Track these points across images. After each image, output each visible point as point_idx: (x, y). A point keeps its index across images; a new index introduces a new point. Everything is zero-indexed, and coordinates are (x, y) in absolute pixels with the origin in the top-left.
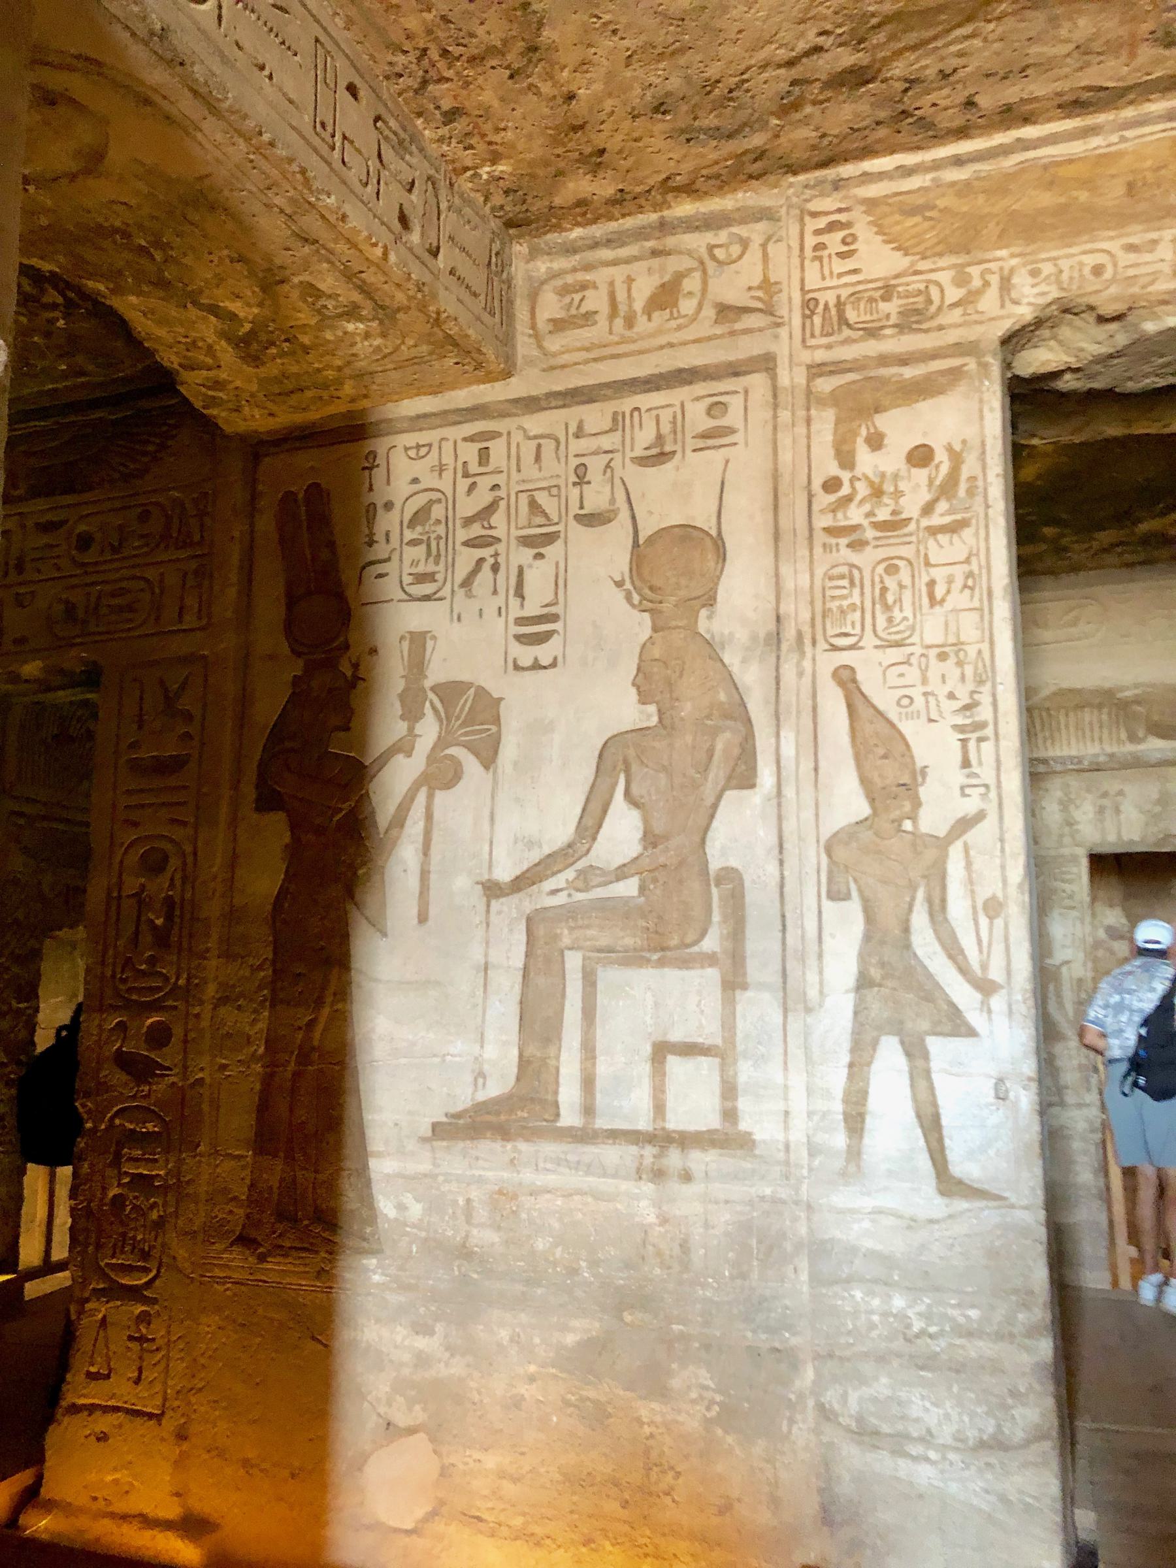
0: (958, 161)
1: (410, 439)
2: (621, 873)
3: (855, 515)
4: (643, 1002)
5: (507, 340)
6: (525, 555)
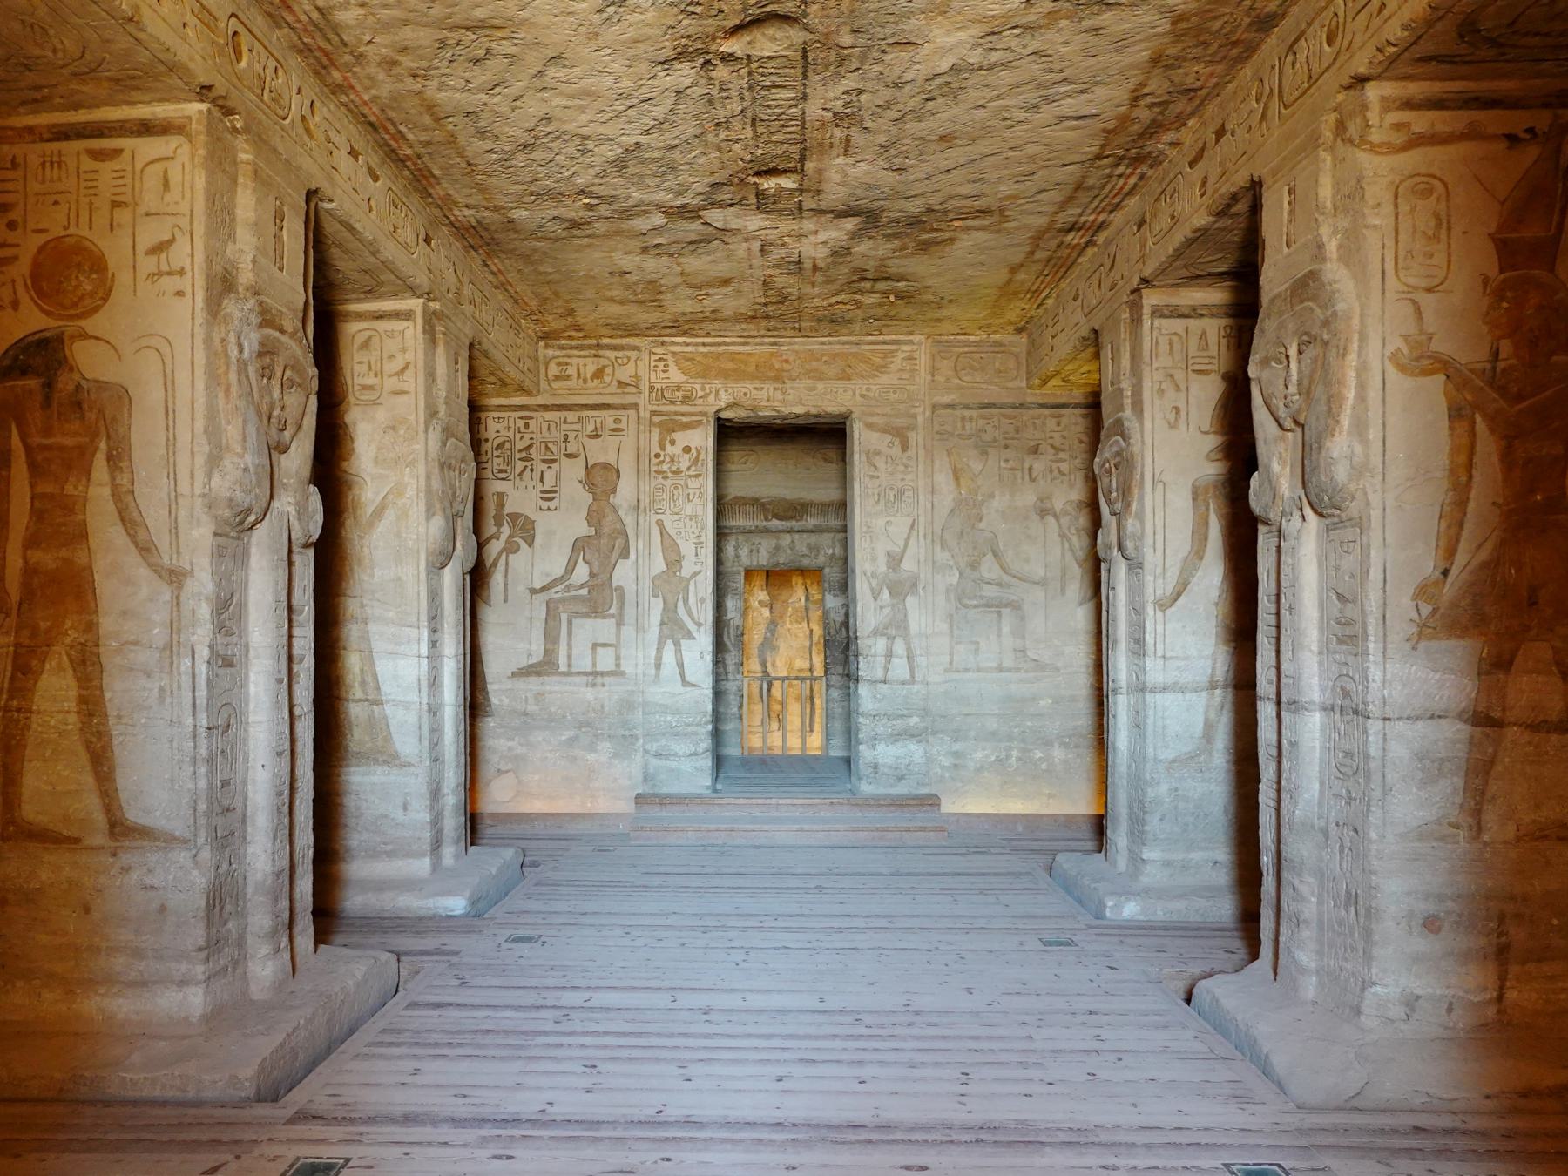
0: (704, 344)
1: (496, 415)
2: (581, 586)
3: (665, 467)
4: (588, 630)
5: (538, 385)
6: (544, 467)
